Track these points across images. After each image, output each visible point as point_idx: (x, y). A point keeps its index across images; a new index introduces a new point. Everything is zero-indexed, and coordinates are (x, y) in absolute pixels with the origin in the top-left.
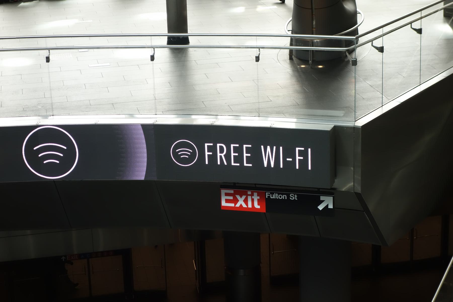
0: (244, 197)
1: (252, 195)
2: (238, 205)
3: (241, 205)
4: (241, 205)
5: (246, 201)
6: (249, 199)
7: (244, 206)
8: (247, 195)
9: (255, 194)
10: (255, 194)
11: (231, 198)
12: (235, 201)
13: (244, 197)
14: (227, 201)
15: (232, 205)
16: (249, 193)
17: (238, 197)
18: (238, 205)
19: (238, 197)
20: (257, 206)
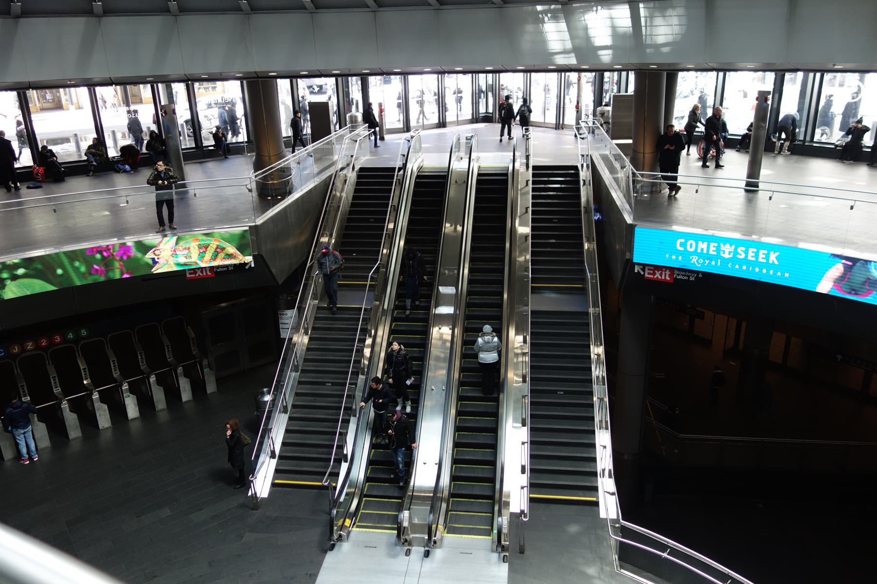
0: (660, 272)
1: (666, 271)
2: (655, 277)
3: (657, 277)
4: (657, 277)
5: (661, 275)
6: (663, 273)
7: (660, 277)
8: (662, 271)
9: (668, 271)
10: (668, 271)
11: (652, 272)
12: (654, 274)
13: (660, 272)
14: (649, 274)
15: (652, 276)
16: (664, 269)
17: (656, 272)
18: (655, 277)
19: (656, 272)
20: (668, 278)
